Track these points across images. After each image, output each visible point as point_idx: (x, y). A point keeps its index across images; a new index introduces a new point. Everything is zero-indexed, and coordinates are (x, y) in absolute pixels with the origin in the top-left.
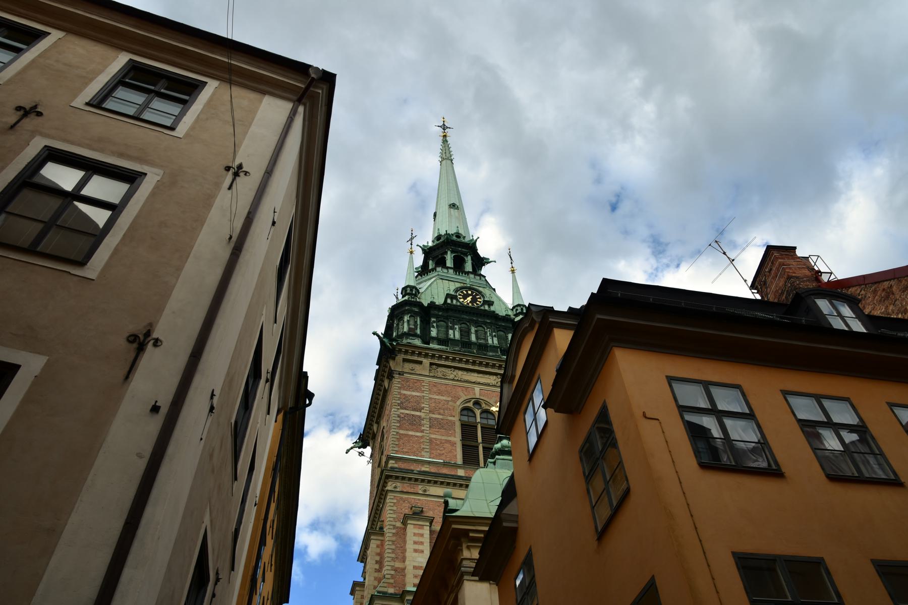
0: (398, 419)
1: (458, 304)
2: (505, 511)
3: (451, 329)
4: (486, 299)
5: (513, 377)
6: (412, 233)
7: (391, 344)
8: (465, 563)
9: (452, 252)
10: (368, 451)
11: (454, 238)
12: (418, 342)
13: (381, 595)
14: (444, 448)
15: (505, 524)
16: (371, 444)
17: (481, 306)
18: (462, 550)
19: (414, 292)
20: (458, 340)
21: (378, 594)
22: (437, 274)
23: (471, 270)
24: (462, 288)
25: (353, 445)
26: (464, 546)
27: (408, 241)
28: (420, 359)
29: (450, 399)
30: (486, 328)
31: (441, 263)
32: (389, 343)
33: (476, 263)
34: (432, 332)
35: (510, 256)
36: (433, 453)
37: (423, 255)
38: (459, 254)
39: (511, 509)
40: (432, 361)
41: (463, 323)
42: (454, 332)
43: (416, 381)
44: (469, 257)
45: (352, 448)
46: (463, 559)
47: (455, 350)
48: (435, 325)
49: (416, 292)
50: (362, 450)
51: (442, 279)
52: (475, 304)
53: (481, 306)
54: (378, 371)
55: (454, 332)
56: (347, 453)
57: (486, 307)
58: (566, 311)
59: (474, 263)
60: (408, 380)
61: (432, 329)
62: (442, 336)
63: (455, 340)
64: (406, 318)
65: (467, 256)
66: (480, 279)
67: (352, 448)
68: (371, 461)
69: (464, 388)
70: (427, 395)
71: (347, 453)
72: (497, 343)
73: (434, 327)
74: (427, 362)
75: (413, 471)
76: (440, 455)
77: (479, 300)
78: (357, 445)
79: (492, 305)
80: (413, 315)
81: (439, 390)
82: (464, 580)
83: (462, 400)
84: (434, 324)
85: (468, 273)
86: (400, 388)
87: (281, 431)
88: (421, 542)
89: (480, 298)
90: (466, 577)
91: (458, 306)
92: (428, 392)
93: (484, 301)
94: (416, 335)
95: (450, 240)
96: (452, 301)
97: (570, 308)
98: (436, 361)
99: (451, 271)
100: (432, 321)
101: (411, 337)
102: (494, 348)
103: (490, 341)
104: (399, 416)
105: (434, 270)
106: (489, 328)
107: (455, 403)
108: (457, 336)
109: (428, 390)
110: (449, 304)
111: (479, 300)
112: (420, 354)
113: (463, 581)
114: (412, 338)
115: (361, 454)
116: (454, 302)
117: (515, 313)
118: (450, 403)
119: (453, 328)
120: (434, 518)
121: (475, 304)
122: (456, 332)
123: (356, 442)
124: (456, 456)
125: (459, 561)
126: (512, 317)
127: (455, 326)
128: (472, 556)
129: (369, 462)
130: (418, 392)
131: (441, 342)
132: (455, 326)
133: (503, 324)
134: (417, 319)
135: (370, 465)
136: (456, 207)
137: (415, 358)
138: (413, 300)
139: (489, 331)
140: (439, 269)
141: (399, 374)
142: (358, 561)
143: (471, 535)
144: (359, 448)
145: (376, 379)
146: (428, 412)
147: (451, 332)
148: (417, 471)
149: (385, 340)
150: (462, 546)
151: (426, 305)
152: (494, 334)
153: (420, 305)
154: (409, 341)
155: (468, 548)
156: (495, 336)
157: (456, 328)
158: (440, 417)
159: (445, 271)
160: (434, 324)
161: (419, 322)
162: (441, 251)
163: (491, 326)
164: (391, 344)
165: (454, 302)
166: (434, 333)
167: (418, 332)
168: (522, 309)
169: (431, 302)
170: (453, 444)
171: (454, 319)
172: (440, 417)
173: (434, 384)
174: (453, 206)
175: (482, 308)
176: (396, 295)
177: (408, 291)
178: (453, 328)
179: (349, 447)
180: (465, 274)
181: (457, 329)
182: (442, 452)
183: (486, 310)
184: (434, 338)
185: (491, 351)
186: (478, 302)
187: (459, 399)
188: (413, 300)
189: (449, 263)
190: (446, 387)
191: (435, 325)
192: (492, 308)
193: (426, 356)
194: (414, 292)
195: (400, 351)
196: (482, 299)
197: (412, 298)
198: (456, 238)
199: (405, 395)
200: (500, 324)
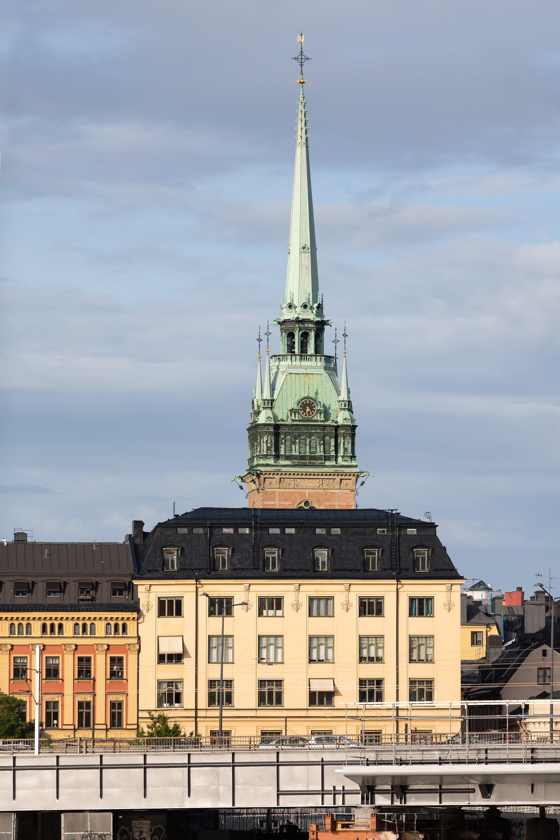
19: (270, 406)
28: (274, 476)
40: (281, 476)
42: (295, 445)
43: (272, 493)
55: (295, 445)
60: (267, 493)
64: (265, 439)
73: (282, 444)
74: (278, 477)
81: (285, 497)
83: (298, 502)
85: (311, 356)
91: (299, 421)
93: (317, 410)
98: (283, 476)
99: (298, 357)
112: (274, 474)
119: (294, 443)
130: (273, 501)
137: (271, 476)
147: (293, 446)
181: (298, 444)
187: (296, 502)
191: (283, 441)
193: (277, 474)
195: (262, 474)
196: (316, 408)
199: (266, 504)
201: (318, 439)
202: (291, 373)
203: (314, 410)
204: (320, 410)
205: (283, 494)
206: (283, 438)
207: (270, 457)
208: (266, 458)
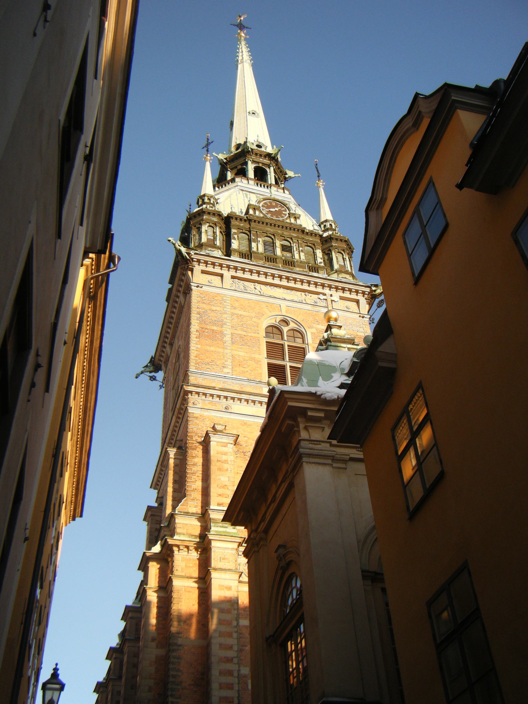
0: (198, 333)
1: (262, 215)
2: (381, 349)
3: (255, 242)
4: (291, 212)
5: (383, 200)
6: (208, 139)
7: (188, 254)
8: (303, 444)
9: (254, 162)
10: (160, 375)
11: (254, 147)
12: (218, 253)
13: (182, 513)
14: (249, 366)
15: (381, 364)
16: (163, 367)
17: (287, 219)
18: (299, 431)
20: (262, 254)
21: (179, 513)
22: (235, 184)
23: (274, 182)
24: (264, 199)
25: (143, 369)
26: (302, 426)
27: (203, 148)
29: (253, 315)
30: (292, 242)
31: (242, 173)
32: (186, 252)
33: (278, 177)
34: (232, 244)
35: (317, 168)
36: (236, 371)
37: (220, 166)
38: (260, 165)
39: (386, 347)
40: (234, 274)
41: (267, 236)
42: (257, 245)
44: (272, 169)
45: (142, 373)
46: (300, 440)
47: (259, 264)
48: (236, 236)
49: (214, 202)
50: (153, 374)
51: (242, 190)
52: (280, 217)
53: (287, 219)
54: (170, 290)
55: (257, 245)
56: (137, 378)
57: (293, 221)
58: (474, 88)
59: (277, 177)
61: (232, 241)
62: (244, 249)
63: (258, 253)
64: (204, 228)
65: (269, 168)
66: (284, 192)
67: (142, 373)
68: (164, 386)
69: (268, 305)
70: (229, 310)
71: (137, 378)
72: (304, 259)
73: (234, 239)
74: (227, 274)
75: (215, 387)
76: (244, 372)
77: (284, 212)
78: (148, 369)
79: (299, 218)
80: (213, 225)
82: (303, 462)
84: (235, 236)
86: (198, 302)
87: (82, 295)
88: (225, 461)
89: (285, 211)
90: (304, 459)
92: (229, 307)
94: (214, 246)
95: (250, 149)
96: (255, 213)
97: (477, 86)
99: (252, 182)
100: (232, 233)
101: (209, 249)
102: (301, 264)
103: (297, 256)
104: (197, 331)
105: (233, 180)
106: (295, 243)
107: (259, 319)
108: (261, 249)
109: (229, 304)
110: (251, 215)
111: (284, 212)
113: (302, 463)
114: (212, 249)
115: (153, 378)
116: (257, 213)
117: (323, 229)
118: (254, 320)
120: (239, 435)
121: (280, 217)
122: (259, 245)
123: (147, 366)
124: (261, 374)
125: (295, 444)
126: (321, 233)
127: (259, 239)
128: (311, 437)
129: (161, 387)
131: (242, 255)
132: (259, 239)
133: (310, 239)
134: (216, 229)
135: (163, 390)
136: (256, 114)
138: (211, 209)
139: (296, 245)
140: (238, 180)
141: (197, 287)
142: (151, 488)
143: (310, 413)
144: (151, 372)
145: (168, 299)
146: (230, 327)
147: (254, 245)
148: (219, 388)
149: (183, 250)
150: (298, 426)
151: (225, 215)
152: (301, 249)
153: (219, 215)
154: (207, 252)
155: (306, 428)
156: (302, 251)
157: (259, 241)
158: (244, 333)
159: (245, 181)
160: (235, 236)
161: (218, 233)
162: (241, 161)
163: (298, 241)
164: (188, 254)
165: (257, 213)
166: (235, 245)
167: (218, 243)
168: (331, 225)
169: (231, 212)
170: (258, 362)
171: (256, 232)
172: (244, 333)
173: (236, 298)
174: (253, 113)
175: (288, 221)
176: (189, 211)
177: (206, 200)
178: (257, 242)
179: (139, 371)
180: (267, 187)
181: (261, 242)
182: (246, 370)
183: (291, 224)
184: (235, 250)
185: (299, 266)
186: (283, 215)
187: (263, 315)
188: (211, 209)
189: (251, 174)
190: (249, 302)
191: (236, 236)
192: (299, 222)
194: (212, 202)
196: (288, 212)
197: (210, 207)
198: (256, 148)
200: (307, 239)
201: (295, 244)
202: (242, 190)
203: (285, 215)
204: (293, 214)
205: (237, 300)
206: (235, 233)
207: (213, 250)
208: (206, 249)
